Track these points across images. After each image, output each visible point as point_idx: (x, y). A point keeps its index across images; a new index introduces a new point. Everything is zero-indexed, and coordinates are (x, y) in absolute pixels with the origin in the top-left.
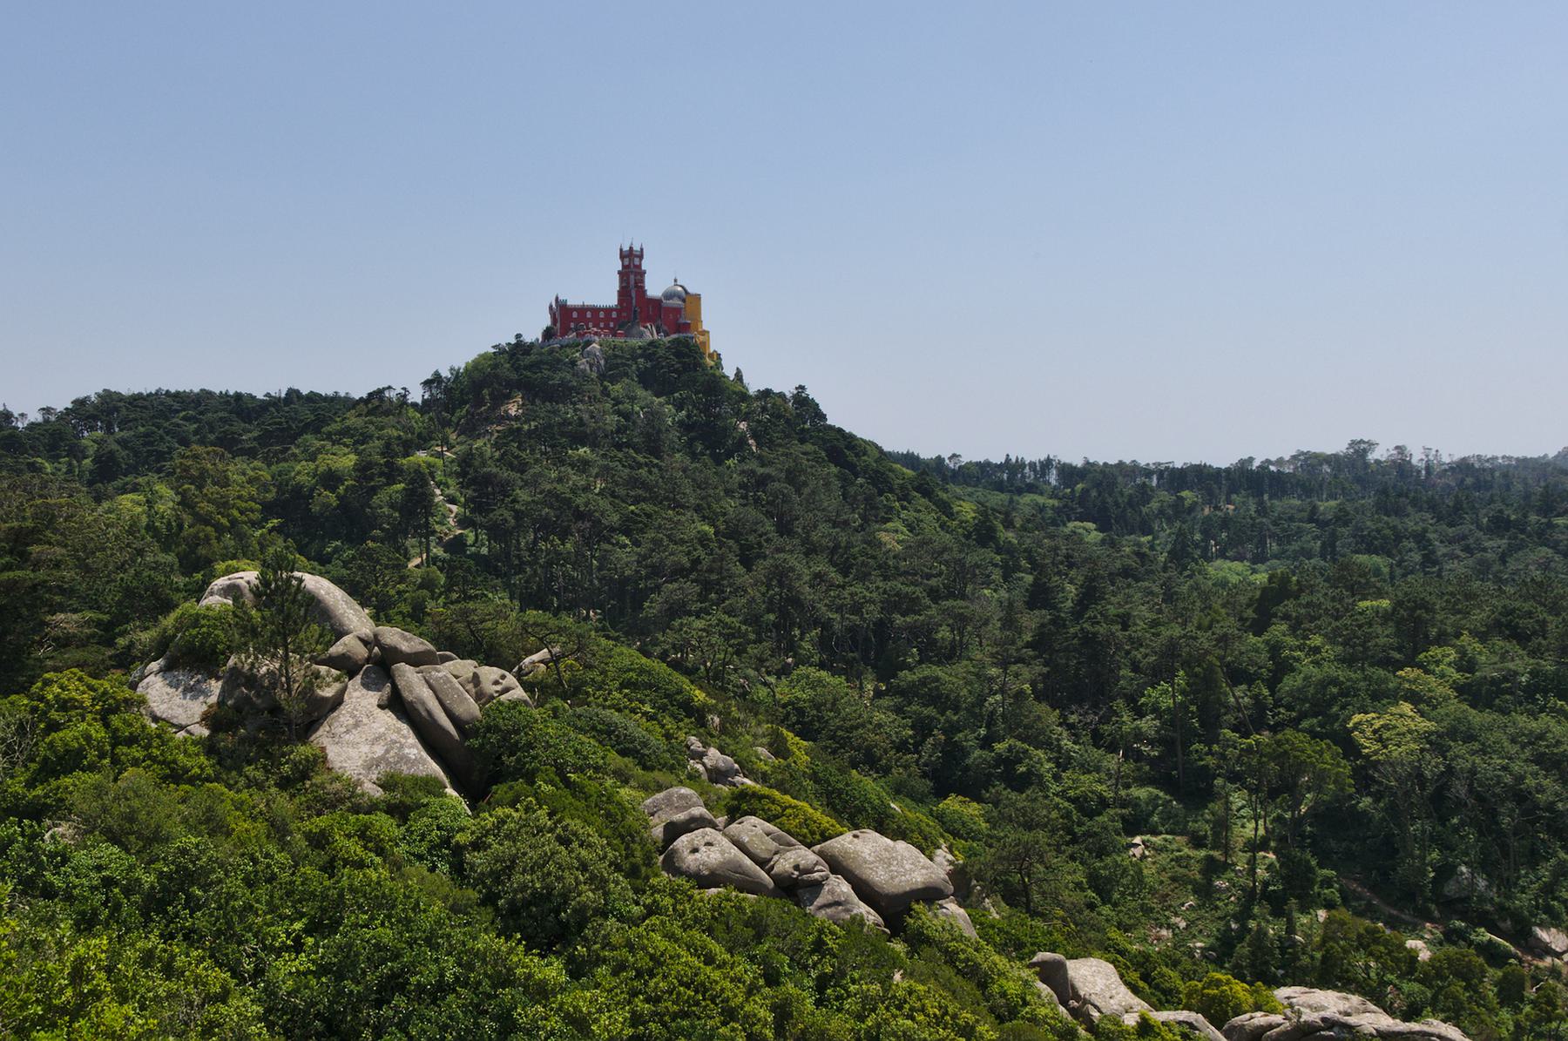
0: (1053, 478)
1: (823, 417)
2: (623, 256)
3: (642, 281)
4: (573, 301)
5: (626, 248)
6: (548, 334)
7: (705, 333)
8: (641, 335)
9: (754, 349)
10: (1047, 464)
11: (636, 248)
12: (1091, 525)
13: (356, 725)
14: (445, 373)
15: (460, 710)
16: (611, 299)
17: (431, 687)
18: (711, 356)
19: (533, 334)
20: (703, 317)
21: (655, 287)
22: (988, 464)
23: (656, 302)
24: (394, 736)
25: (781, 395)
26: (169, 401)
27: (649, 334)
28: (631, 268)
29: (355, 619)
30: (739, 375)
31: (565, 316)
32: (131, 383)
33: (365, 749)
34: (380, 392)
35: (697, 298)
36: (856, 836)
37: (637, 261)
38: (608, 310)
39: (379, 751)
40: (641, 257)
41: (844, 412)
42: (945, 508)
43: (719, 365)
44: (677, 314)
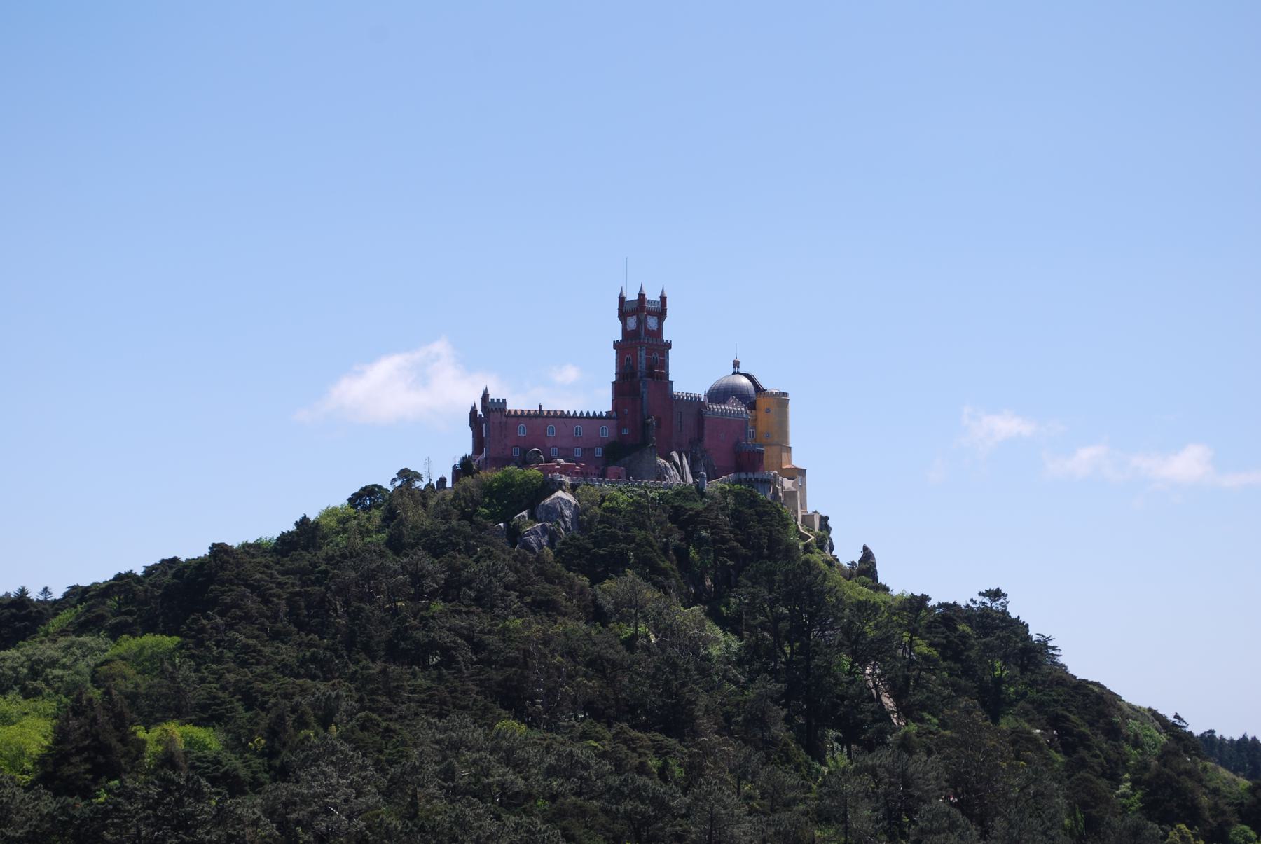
2: (626, 310)
3: (664, 364)
5: (631, 296)
6: (464, 469)
8: (661, 474)
9: (900, 508)
11: (652, 296)
16: (602, 402)
18: (807, 520)
20: (793, 440)
23: (693, 404)
27: (677, 473)
28: (642, 337)
37: (652, 323)
40: (661, 313)
43: (824, 541)
44: (743, 430)
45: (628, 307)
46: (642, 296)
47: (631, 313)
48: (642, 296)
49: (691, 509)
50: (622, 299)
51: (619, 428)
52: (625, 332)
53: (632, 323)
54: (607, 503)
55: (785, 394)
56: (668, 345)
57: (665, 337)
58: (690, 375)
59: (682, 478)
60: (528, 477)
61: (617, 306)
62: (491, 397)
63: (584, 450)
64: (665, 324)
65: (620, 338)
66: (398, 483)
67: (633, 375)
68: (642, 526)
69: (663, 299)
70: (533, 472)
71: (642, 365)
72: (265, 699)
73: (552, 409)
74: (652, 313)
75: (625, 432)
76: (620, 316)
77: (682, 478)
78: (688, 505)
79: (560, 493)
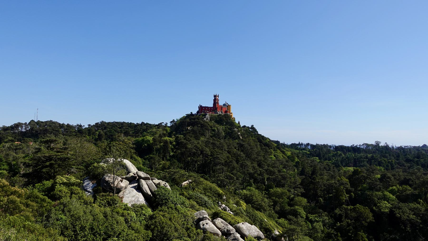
0: (309, 147)
1: (257, 132)
6: (198, 112)
7: (231, 113)
9: (242, 117)
10: (308, 144)
11: (217, 95)
12: (318, 158)
13: (129, 193)
14: (176, 120)
15: (153, 190)
16: (212, 106)
17: (147, 185)
19: (194, 112)
21: (221, 103)
22: (295, 144)
24: (137, 196)
25: (248, 127)
26: (116, 124)
28: (216, 100)
29: (133, 169)
30: (239, 123)
31: (202, 109)
32: (108, 120)
33: (130, 198)
34: (161, 123)
35: (230, 106)
36: (243, 224)
38: (211, 108)
39: (133, 199)
41: (261, 131)
42: (283, 152)
58: (221, 103)
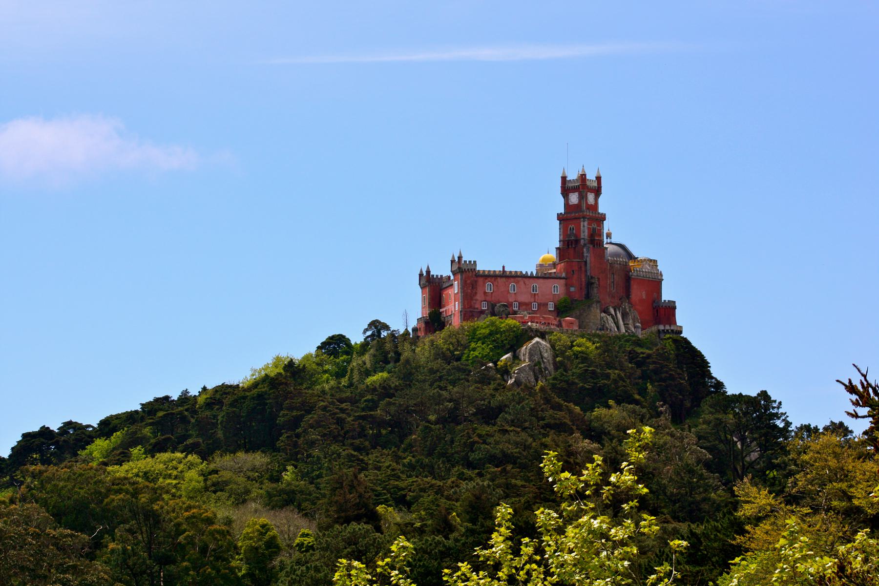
2: (566, 188)
4: (487, 263)
5: (572, 176)
11: (591, 176)
37: (591, 197)
45: (570, 185)
46: (583, 177)
47: (574, 189)
48: (583, 177)
49: (643, 353)
50: (564, 178)
51: (567, 286)
52: (567, 205)
53: (574, 198)
54: (576, 348)
55: (655, 261)
56: (603, 218)
57: (601, 210)
59: (618, 328)
60: (510, 326)
61: (560, 185)
62: (464, 259)
63: (539, 305)
64: (601, 200)
65: (562, 210)
66: (369, 333)
67: (577, 241)
68: (610, 366)
69: (599, 179)
70: (510, 322)
71: (585, 234)
72: (403, 492)
73: (513, 270)
74: (592, 190)
75: (572, 289)
76: (562, 194)
77: (618, 328)
78: (639, 350)
79: (537, 339)
